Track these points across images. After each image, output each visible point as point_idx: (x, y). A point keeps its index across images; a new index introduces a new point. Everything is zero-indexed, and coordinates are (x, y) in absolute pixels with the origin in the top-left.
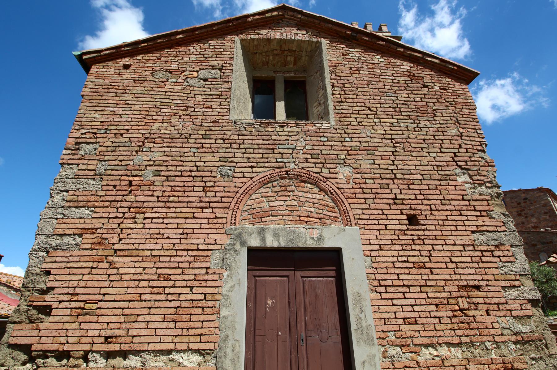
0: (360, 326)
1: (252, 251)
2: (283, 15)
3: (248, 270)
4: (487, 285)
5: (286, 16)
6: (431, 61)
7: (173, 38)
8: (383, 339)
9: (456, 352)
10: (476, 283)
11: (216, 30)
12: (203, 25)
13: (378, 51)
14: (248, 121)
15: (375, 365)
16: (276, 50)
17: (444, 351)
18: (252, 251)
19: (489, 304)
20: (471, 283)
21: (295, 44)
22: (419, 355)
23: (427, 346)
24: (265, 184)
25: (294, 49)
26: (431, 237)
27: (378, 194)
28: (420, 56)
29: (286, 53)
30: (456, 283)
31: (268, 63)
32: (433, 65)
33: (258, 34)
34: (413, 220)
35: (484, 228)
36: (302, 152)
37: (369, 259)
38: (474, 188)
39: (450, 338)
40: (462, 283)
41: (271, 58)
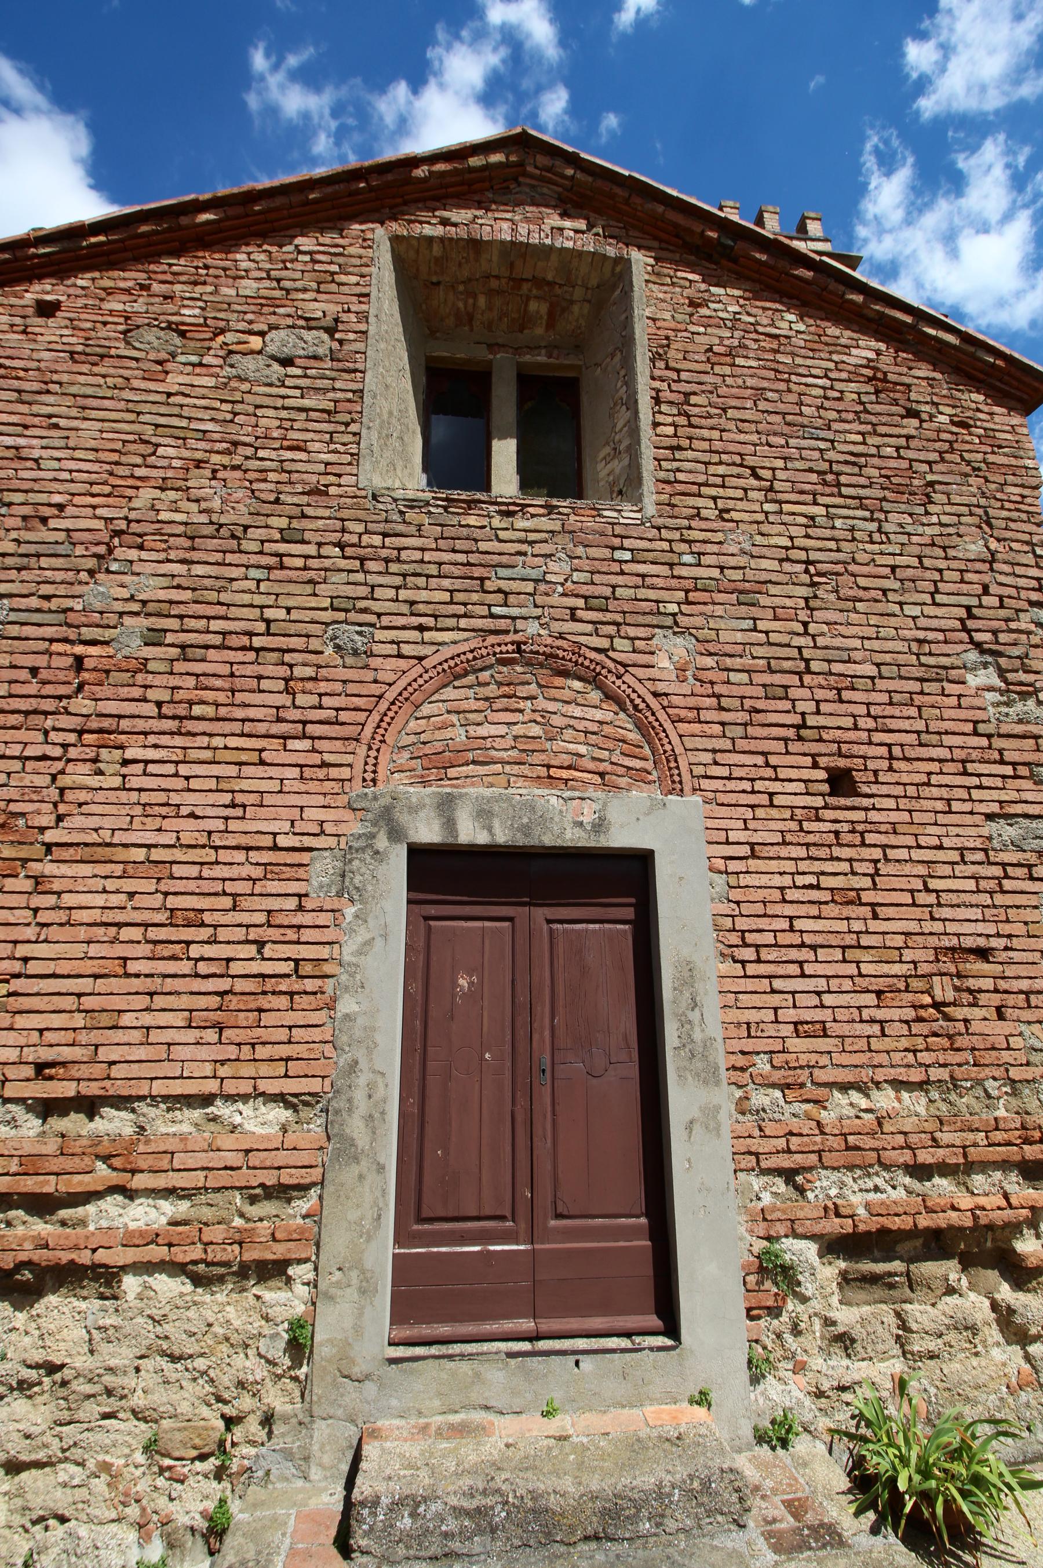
0: (687, 1040)
1: (418, 854)
2: (520, 164)
3: (409, 902)
4: (1006, 949)
5: (530, 169)
6: (935, 338)
7: (184, 220)
8: (743, 1069)
9: (915, 1103)
10: (981, 942)
11: (315, 201)
12: (276, 182)
13: (790, 297)
14: (411, 494)
15: (718, 1129)
16: (497, 277)
17: (885, 1099)
18: (418, 854)
19: (1006, 992)
20: (969, 942)
21: (554, 257)
22: (825, 1108)
23: (845, 1087)
24: (457, 677)
25: (550, 277)
26: (883, 828)
27: (758, 711)
28: (908, 319)
29: (526, 286)
30: (933, 941)
31: (471, 318)
32: (939, 351)
33: (445, 222)
34: (841, 782)
35: (1018, 809)
36: (560, 589)
37: (720, 880)
38: (1006, 704)
39: (902, 1070)
40: (946, 942)
41: (482, 301)
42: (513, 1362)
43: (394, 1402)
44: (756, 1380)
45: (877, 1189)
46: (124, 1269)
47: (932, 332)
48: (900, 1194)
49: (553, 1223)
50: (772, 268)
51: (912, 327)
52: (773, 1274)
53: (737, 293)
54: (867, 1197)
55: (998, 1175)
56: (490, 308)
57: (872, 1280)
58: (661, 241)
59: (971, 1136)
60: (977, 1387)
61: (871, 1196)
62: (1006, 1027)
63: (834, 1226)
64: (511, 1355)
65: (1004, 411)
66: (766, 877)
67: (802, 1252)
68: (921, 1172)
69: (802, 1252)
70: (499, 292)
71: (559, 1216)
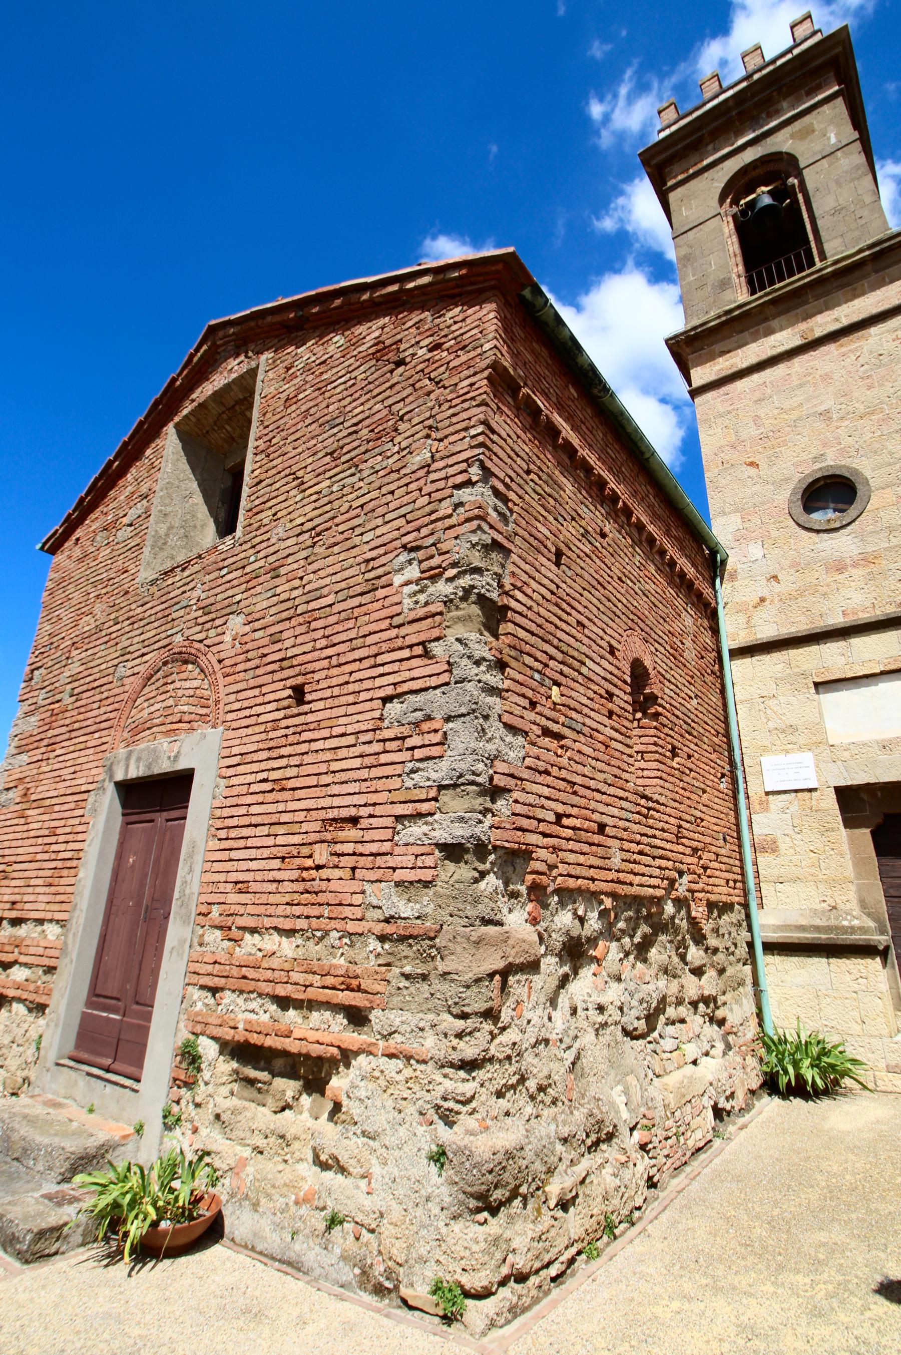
0: (183, 892)
1: (118, 785)
2: (214, 343)
3: (124, 815)
4: (371, 816)
5: (219, 343)
6: (416, 288)
7: (110, 471)
8: (205, 915)
9: (287, 947)
10: (353, 812)
11: (149, 427)
12: (131, 431)
13: (339, 323)
14: (151, 578)
15: (182, 954)
16: (223, 413)
17: (271, 942)
18: (118, 785)
19: (361, 855)
20: (345, 813)
21: (233, 387)
22: (239, 946)
23: (253, 931)
24: (149, 679)
25: (241, 397)
26: (312, 726)
27: (265, 655)
28: (395, 288)
29: (237, 408)
30: (322, 814)
31: (233, 439)
32: (424, 294)
33: (193, 401)
34: (299, 694)
35: (405, 687)
36: (194, 607)
37: (223, 783)
38: (422, 591)
39: (282, 919)
40: (331, 814)
41: (227, 427)
42: (88, 1078)
43: (53, 1086)
44: (168, 1127)
45: (253, 1011)
46: (14, 998)
47: (411, 285)
48: (265, 1018)
49: (135, 1007)
50: (324, 312)
51: (401, 290)
52: (190, 1057)
53: (313, 341)
54: (250, 1015)
55: (328, 1014)
56: (234, 429)
57: (251, 1082)
58: (276, 336)
59: (310, 977)
60: (274, 1186)
61: (253, 1017)
62: (355, 886)
63: (227, 1034)
64: (89, 1074)
65: (478, 307)
66: (247, 775)
67: (208, 1049)
68: (284, 1003)
69: (208, 1049)
70: (230, 419)
71: (138, 1003)
